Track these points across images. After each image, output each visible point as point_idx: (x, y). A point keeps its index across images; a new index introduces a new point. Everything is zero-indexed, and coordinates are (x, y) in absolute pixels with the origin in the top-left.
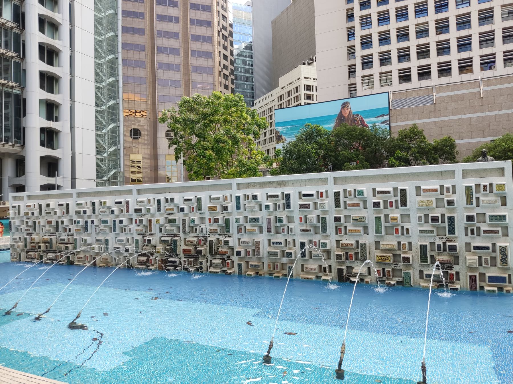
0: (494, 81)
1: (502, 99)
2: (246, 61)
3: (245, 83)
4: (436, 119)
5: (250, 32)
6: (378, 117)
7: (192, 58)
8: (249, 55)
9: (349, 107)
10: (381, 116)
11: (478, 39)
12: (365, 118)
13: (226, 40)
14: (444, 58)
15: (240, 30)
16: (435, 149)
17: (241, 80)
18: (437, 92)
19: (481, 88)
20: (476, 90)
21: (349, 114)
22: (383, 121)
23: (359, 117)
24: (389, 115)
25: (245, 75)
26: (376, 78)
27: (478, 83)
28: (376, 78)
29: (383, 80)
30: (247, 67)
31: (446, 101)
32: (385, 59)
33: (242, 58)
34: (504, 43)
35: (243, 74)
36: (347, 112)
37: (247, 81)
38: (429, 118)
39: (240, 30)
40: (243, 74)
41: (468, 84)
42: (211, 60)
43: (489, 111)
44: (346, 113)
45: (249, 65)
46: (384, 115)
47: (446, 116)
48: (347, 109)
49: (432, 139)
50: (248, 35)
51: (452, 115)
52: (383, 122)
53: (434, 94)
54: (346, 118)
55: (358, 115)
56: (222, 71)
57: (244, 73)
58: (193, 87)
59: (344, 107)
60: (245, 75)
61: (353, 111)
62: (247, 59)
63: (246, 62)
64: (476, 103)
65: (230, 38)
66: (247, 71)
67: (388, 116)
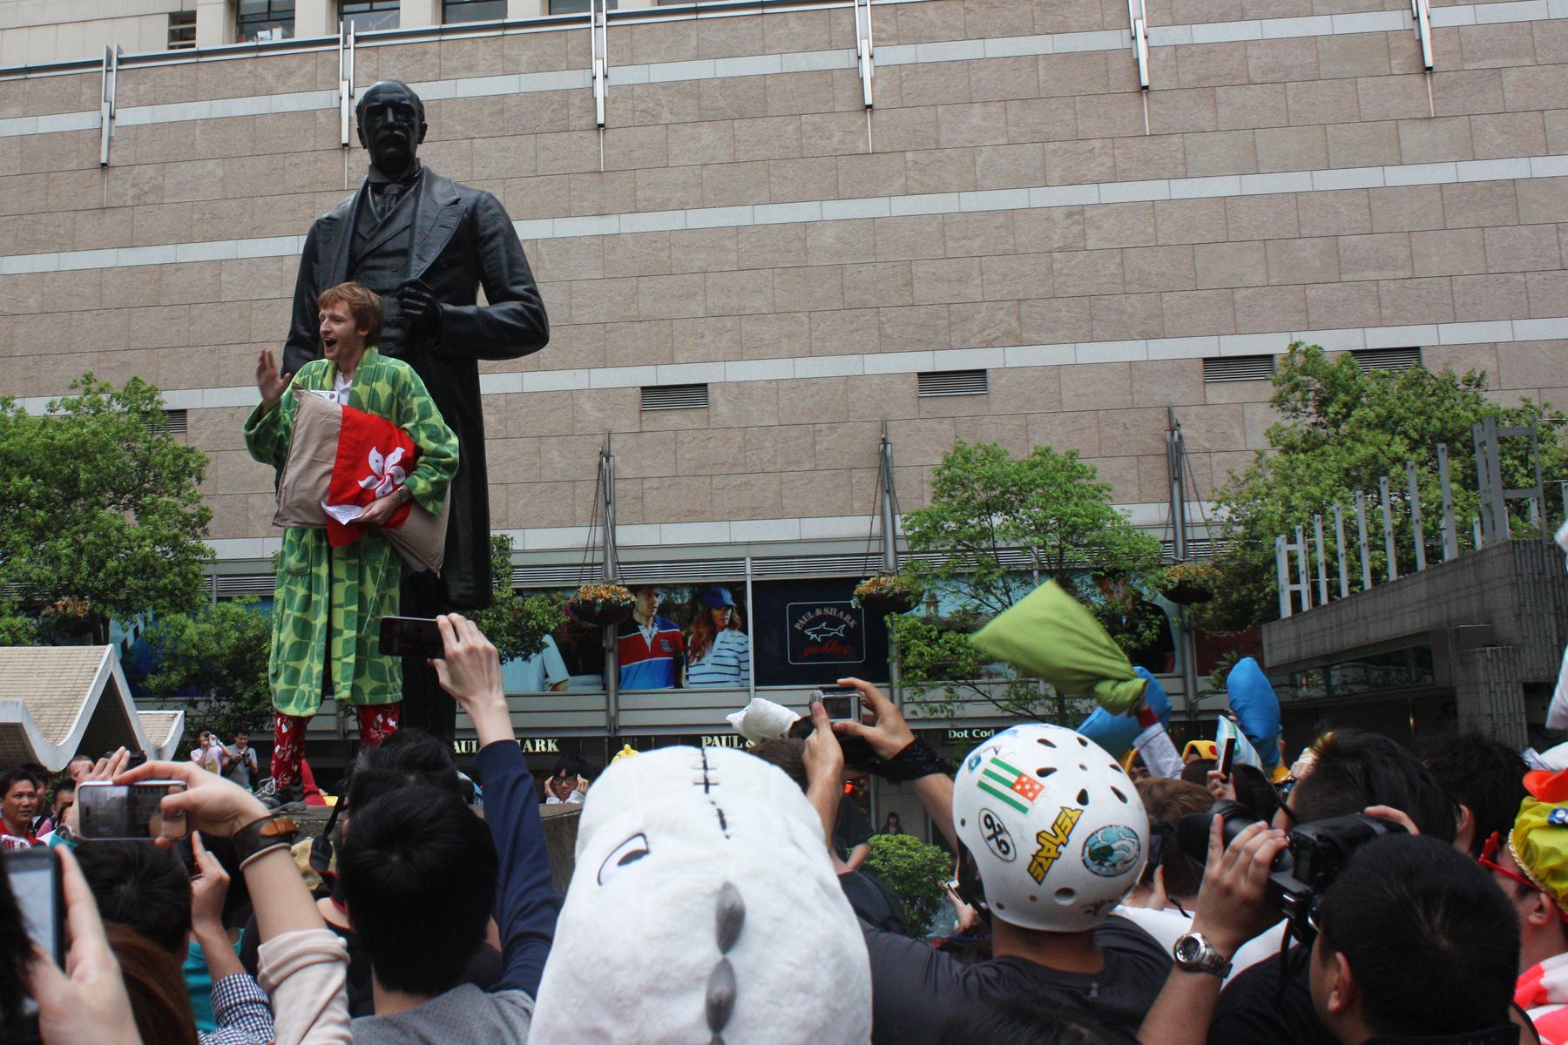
1: (975, 121)
4: (609, 225)
18: (618, 58)
20: (835, 60)
27: (846, 20)
31: (666, 117)
38: (568, 213)
41: (793, 23)
43: (907, 192)
51: (702, 204)
64: (836, 139)
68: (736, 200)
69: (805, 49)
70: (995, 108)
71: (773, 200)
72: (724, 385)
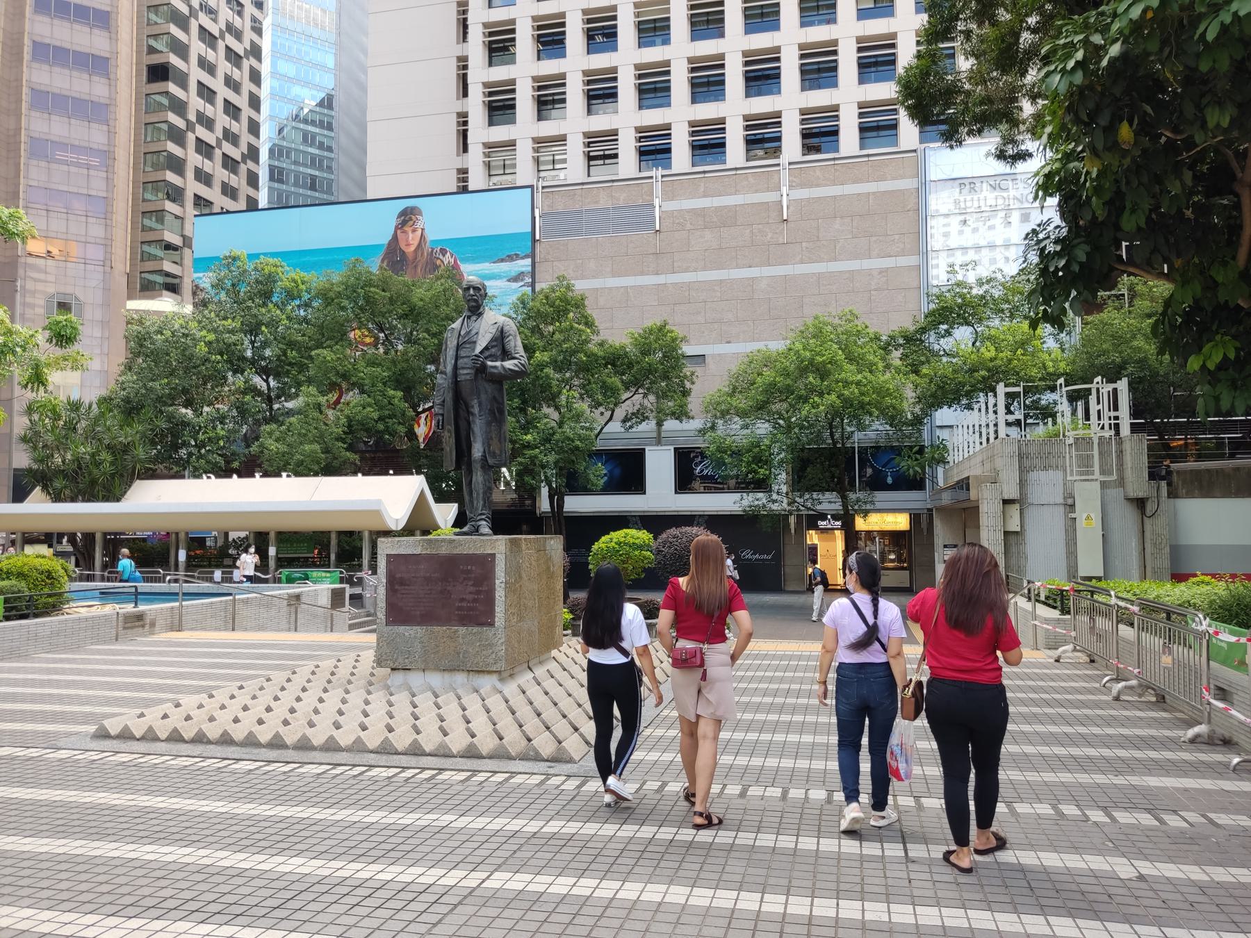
0: (818, 173)
1: (837, 226)
2: (314, 136)
3: (309, 193)
4: (661, 279)
5: (330, 62)
6: (502, 260)
7: (35, 65)
8: (321, 122)
9: (419, 225)
10: (511, 258)
11: (855, 122)
12: (465, 260)
13: (238, 65)
14: (707, 111)
15: (299, 51)
16: (615, 360)
17: (296, 184)
18: (667, 196)
19: (784, 190)
20: (770, 197)
21: (419, 245)
22: (514, 274)
23: (448, 259)
24: (533, 256)
25: (309, 171)
26: (524, 152)
27: (776, 176)
28: (524, 152)
29: (546, 163)
30: (317, 152)
31: (688, 226)
33: (301, 126)
34: (861, 82)
35: (301, 169)
36: (413, 239)
37: (313, 188)
38: (642, 273)
39: (299, 51)
40: (301, 169)
41: (751, 179)
42: (104, 80)
44: (410, 242)
45: (321, 146)
46: (517, 257)
47: (686, 270)
48: (414, 231)
49: (616, 330)
50: (322, 67)
51: (704, 269)
52: (516, 279)
53: (657, 202)
54: (410, 257)
55: (443, 252)
56: (219, 145)
57: (305, 165)
58: (33, 154)
59: (404, 223)
60: (309, 171)
61: (430, 236)
62: (317, 130)
63: (314, 138)
64: (770, 235)
65: (253, 62)
66: (314, 162)
68: (720, 267)
69: (756, 191)
70: (847, 220)
71: (738, 267)
72: (713, 356)
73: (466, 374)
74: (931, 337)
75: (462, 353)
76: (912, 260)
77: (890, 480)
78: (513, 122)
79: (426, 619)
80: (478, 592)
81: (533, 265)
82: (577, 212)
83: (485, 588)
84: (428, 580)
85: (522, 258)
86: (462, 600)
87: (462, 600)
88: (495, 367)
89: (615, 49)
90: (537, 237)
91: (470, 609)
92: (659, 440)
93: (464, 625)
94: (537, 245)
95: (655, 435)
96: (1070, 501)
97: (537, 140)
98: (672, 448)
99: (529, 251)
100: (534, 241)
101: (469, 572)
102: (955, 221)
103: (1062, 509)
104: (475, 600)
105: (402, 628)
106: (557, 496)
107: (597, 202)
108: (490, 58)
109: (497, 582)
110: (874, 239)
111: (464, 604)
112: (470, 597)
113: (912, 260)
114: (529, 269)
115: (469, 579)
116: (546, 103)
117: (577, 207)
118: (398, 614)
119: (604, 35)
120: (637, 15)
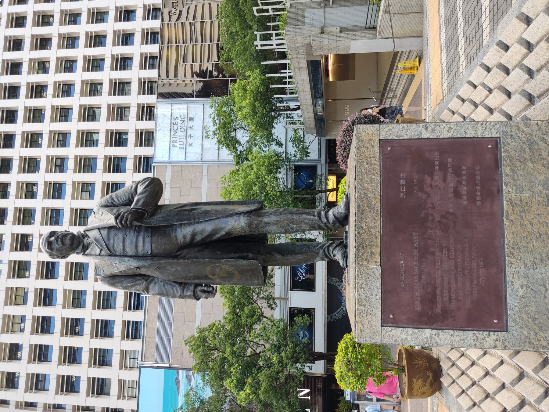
6: (178, 388)
10: (177, 383)
22: (186, 382)
24: (178, 369)
32: (102, 358)
46: (177, 379)
52: (189, 380)
67: (181, 372)
73: (145, 245)
74: (240, 149)
75: (119, 249)
76: (205, 168)
77: (311, 181)
78: (110, 380)
79: (492, 256)
80: (443, 167)
81: (183, 369)
82: (158, 342)
83: (436, 156)
84: (424, 252)
85: (178, 375)
86: (457, 193)
87: (457, 193)
88: (138, 201)
89: (83, 320)
90: (168, 365)
91: (471, 178)
92: (285, 299)
93: (499, 191)
94: (172, 366)
95: (282, 301)
96: (323, 5)
97: (121, 368)
98: (290, 292)
99: (175, 371)
100: (170, 368)
101: (409, 183)
102: (190, 149)
103: (327, 9)
104: (457, 172)
105: (512, 302)
106: (314, 357)
107: (154, 329)
108: (75, 392)
109: (425, 135)
110: (193, 186)
111: (464, 190)
112: (451, 180)
113: (205, 168)
114: (185, 371)
115: (421, 182)
116: (103, 361)
117: (155, 341)
118: (485, 312)
119: (76, 325)
120: (69, 307)
